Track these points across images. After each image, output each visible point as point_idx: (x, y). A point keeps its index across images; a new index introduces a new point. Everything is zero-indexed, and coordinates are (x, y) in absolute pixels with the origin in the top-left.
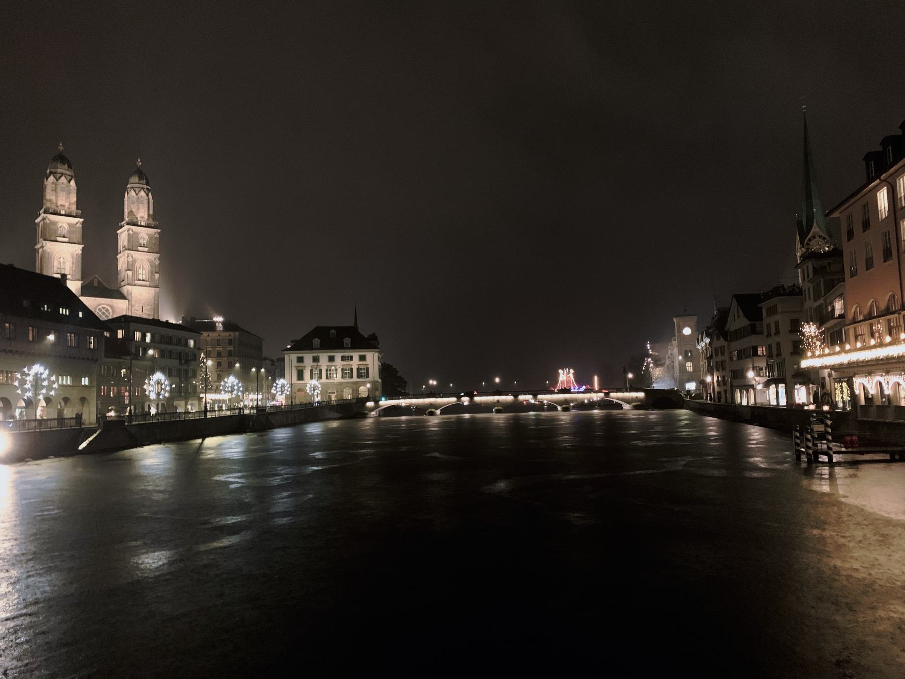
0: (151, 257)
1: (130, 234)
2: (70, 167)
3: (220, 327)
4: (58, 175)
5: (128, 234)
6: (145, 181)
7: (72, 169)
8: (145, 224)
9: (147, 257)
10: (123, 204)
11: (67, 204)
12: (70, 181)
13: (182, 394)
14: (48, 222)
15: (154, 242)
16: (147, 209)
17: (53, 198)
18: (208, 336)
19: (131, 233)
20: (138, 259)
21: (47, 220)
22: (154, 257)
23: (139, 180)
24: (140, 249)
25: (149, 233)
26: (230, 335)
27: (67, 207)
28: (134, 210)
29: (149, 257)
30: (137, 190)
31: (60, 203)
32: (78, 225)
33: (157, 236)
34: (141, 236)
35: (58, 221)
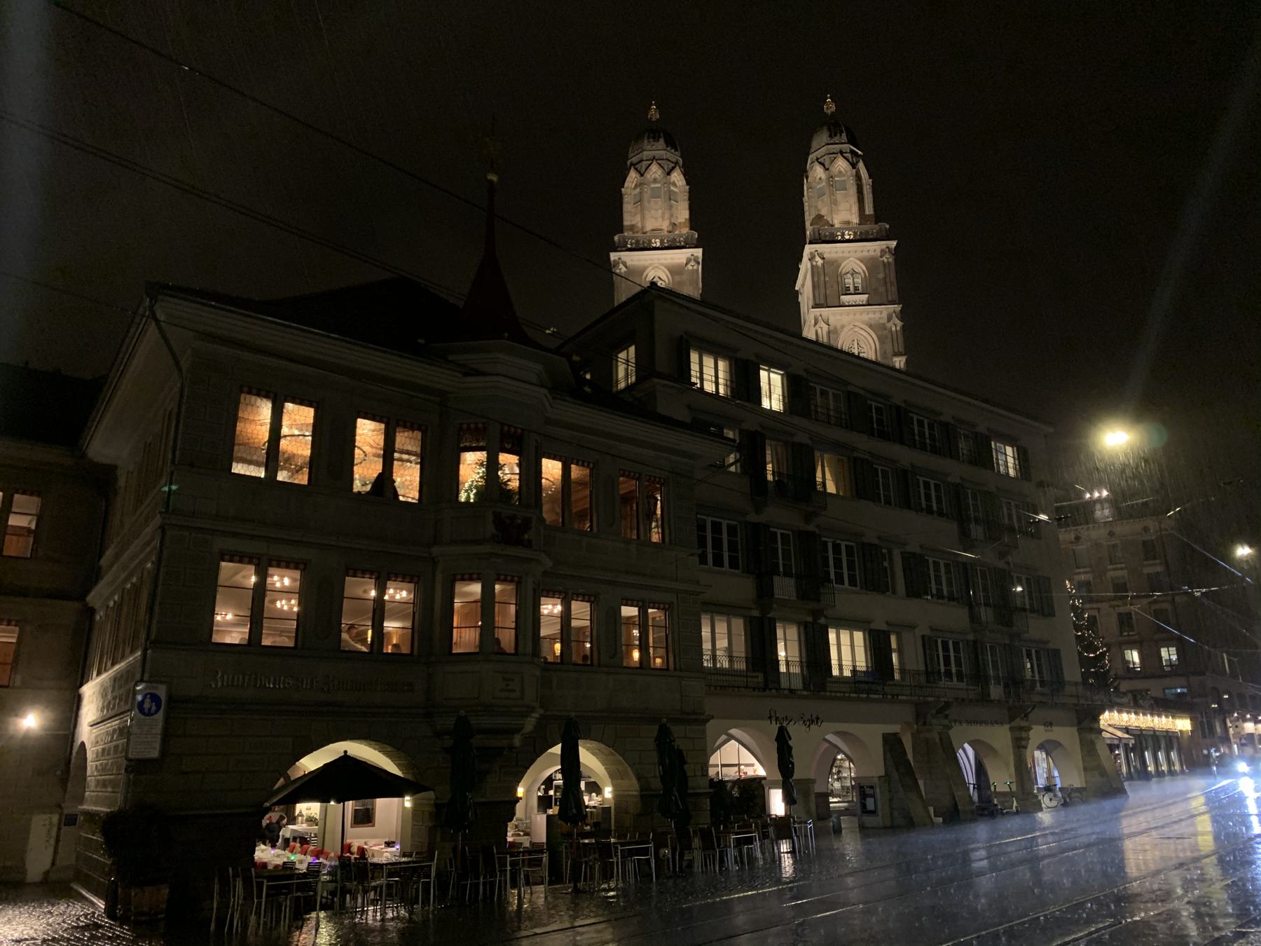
0: (878, 315)
1: (817, 266)
2: (671, 143)
3: (1103, 513)
4: (645, 164)
5: (812, 266)
6: (844, 135)
7: (676, 150)
8: (855, 234)
9: (865, 317)
10: (803, 205)
11: (665, 225)
12: (669, 174)
13: (996, 691)
14: (624, 269)
15: (881, 276)
16: (853, 200)
17: (637, 220)
18: (1077, 538)
19: (820, 262)
20: (843, 327)
21: (621, 266)
22: (885, 315)
23: (830, 136)
24: (845, 299)
25: (866, 254)
26: (1146, 529)
27: (666, 229)
28: (824, 212)
29: (871, 316)
30: (827, 160)
31: (648, 227)
32: (689, 267)
33: (888, 258)
34: (846, 266)
35: (647, 263)
